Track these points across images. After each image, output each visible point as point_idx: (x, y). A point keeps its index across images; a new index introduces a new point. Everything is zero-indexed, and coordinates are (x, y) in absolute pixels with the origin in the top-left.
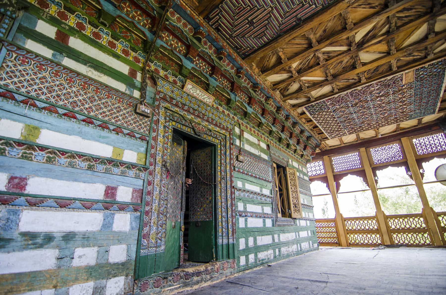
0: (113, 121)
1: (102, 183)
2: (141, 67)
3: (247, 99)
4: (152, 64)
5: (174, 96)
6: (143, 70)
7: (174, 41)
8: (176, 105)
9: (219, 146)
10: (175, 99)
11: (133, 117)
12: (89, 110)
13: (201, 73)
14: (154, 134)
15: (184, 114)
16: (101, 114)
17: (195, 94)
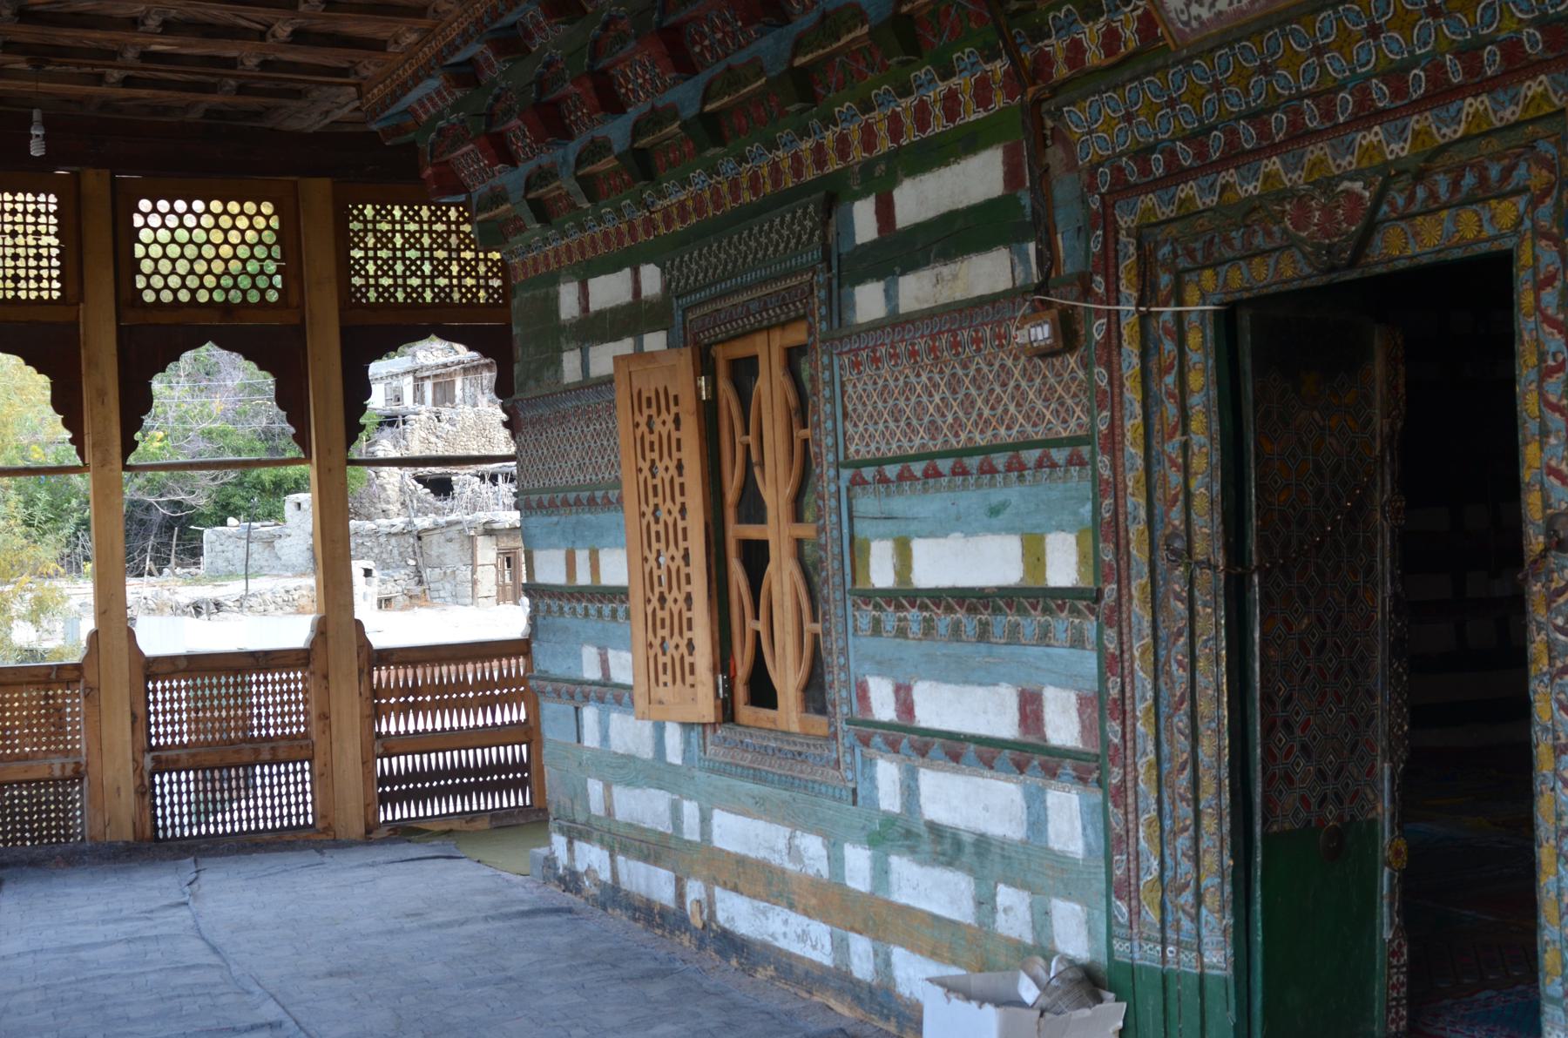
1: (1011, 680)
4: (1053, 40)
5: (1143, 133)
8: (1175, 174)
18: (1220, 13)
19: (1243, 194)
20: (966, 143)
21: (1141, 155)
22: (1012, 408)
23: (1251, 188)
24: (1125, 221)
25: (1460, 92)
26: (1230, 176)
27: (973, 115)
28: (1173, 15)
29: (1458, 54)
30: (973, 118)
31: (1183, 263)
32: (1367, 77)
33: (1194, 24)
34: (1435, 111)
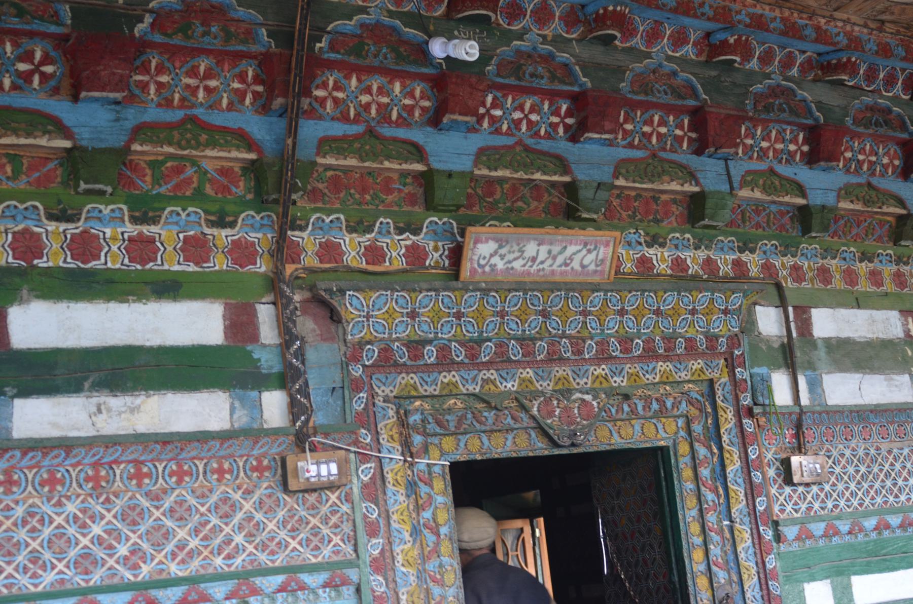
0: (219, 561)
2: (264, 275)
3: (794, 141)
4: (305, 234)
5: (424, 330)
6: (274, 284)
7: (368, 90)
8: (445, 362)
9: (684, 448)
10: (430, 342)
11: (281, 514)
12: (134, 559)
13: (527, 149)
14: (373, 547)
15: (486, 381)
16: (174, 555)
17: (517, 265)
18: (512, 268)
19: (503, 388)
20: (168, 288)
21: (415, 346)
22: (239, 539)
23: (509, 385)
24: (382, 391)
25: (657, 357)
26: (492, 374)
27: (172, 263)
28: (476, 258)
29: (663, 338)
30: (176, 268)
31: (432, 427)
32: (610, 336)
33: (487, 269)
34: (641, 365)
